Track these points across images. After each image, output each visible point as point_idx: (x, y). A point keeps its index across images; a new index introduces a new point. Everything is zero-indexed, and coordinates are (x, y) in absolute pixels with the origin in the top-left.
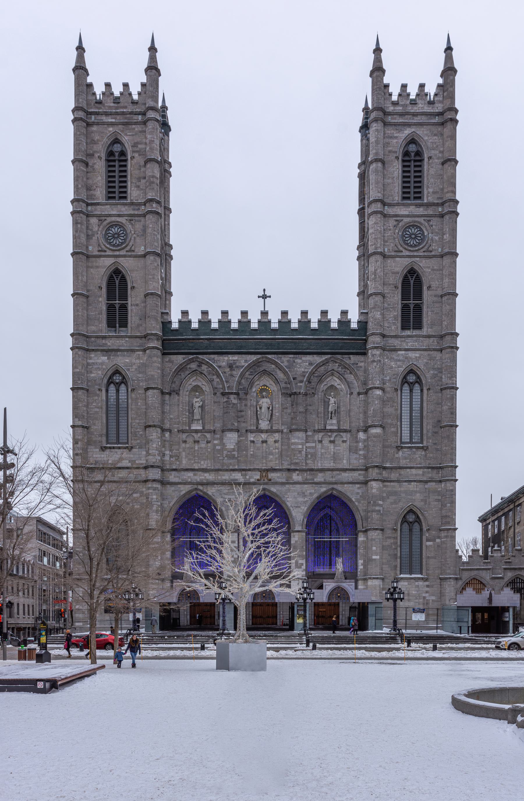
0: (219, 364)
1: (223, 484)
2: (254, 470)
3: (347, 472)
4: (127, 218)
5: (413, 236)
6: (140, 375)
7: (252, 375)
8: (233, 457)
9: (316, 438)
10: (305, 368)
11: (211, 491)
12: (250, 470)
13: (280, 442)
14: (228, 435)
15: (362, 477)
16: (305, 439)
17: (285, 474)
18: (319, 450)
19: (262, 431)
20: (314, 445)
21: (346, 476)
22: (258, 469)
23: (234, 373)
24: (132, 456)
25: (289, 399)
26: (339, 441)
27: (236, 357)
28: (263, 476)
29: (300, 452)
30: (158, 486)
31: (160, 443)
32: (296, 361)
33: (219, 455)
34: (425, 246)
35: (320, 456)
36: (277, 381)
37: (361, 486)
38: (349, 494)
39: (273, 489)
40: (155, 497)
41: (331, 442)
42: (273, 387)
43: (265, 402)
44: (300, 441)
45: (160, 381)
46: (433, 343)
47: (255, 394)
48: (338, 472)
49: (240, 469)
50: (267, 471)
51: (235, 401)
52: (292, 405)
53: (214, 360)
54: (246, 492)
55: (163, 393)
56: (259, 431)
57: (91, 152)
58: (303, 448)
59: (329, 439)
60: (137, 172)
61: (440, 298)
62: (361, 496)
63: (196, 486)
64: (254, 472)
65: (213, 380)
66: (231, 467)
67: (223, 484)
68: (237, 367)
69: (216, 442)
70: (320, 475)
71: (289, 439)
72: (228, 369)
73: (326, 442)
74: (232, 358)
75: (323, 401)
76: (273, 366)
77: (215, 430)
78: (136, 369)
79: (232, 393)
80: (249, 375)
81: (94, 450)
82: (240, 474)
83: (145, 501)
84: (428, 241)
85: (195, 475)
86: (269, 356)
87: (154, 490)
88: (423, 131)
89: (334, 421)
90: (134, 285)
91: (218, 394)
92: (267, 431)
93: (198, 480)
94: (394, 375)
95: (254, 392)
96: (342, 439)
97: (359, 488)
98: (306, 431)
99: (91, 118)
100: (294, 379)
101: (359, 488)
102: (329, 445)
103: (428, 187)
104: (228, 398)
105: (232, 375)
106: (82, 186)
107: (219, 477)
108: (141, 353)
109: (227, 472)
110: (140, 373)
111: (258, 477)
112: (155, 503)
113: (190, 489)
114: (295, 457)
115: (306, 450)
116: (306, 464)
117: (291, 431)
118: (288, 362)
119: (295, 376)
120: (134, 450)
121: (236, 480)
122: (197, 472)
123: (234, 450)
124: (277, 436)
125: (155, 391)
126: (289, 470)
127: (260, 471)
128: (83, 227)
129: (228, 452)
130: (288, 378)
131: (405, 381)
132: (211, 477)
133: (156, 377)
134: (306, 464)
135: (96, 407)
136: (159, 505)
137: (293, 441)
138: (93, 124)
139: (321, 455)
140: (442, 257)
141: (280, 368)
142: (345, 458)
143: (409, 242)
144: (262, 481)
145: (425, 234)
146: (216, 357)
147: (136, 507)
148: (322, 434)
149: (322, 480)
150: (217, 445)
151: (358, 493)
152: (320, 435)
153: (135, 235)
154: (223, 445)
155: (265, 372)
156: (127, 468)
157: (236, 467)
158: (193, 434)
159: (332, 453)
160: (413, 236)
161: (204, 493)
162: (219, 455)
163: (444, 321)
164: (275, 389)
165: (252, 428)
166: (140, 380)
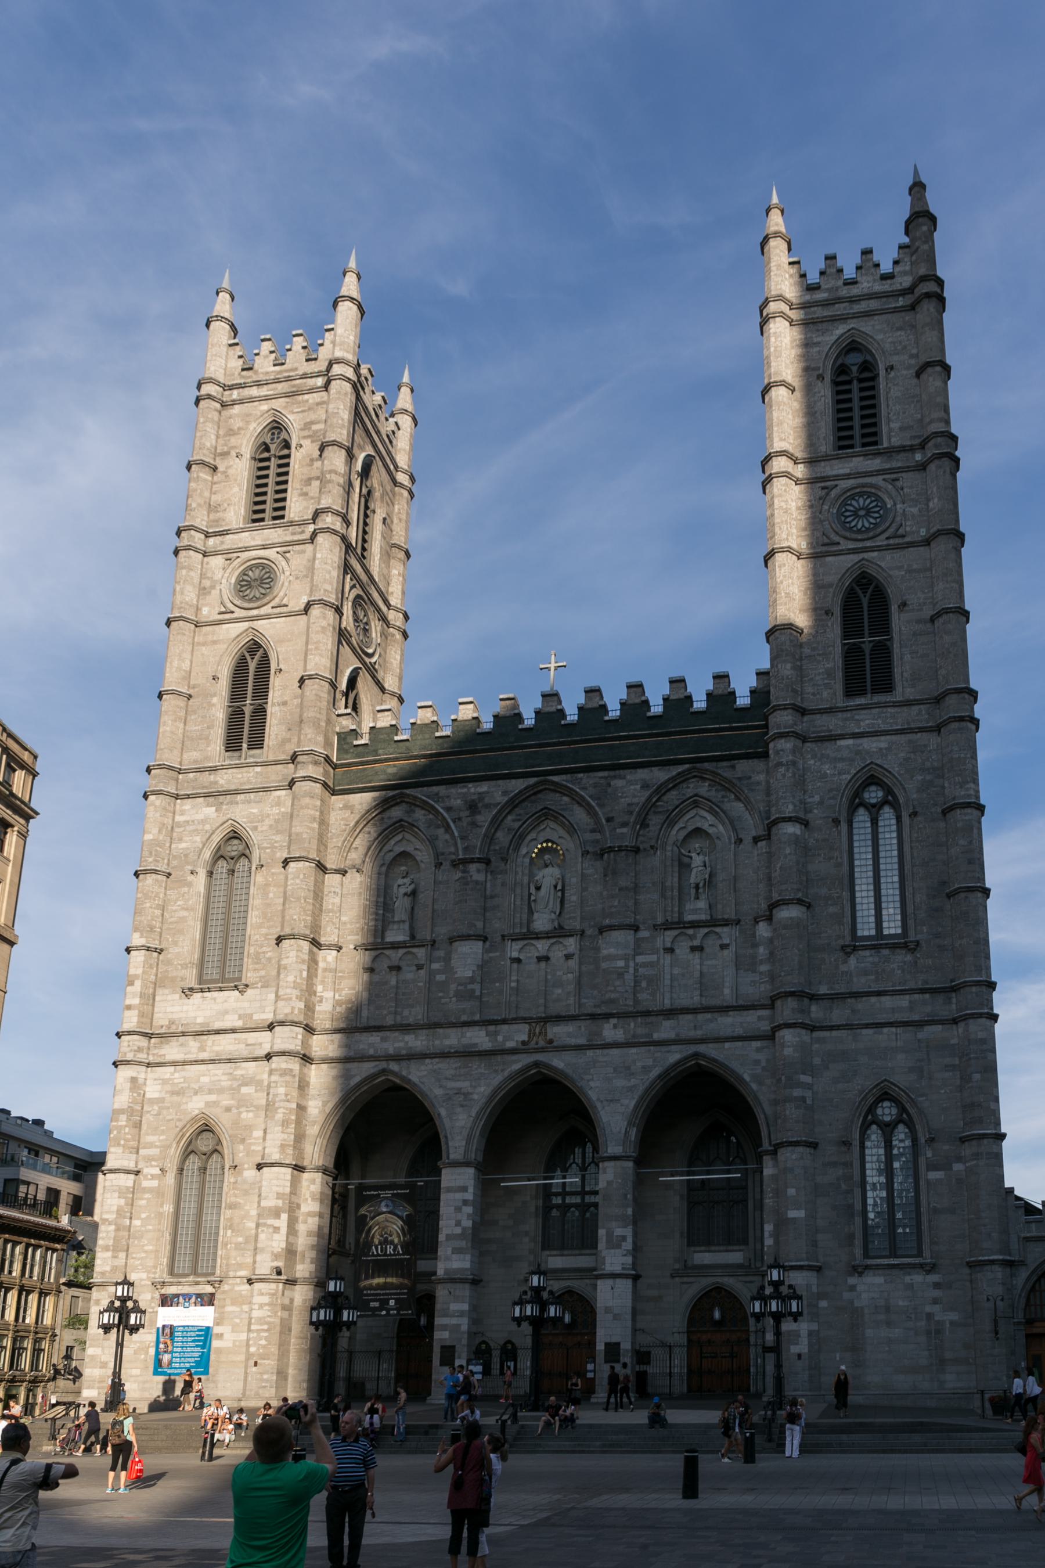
0: (448, 804)
1: (444, 1055)
2: (515, 1020)
3: (731, 1013)
4: (278, 549)
5: (862, 513)
6: (278, 838)
7: (519, 820)
8: (470, 995)
9: (659, 943)
10: (634, 796)
11: (417, 1075)
12: (504, 1021)
13: (576, 957)
14: (459, 949)
15: (767, 1022)
16: (632, 946)
17: (584, 1025)
18: (667, 969)
19: (538, 936)
20: (654, 958)
21: (728, 1024)
22: (524, 1019)
23: (479, 818)
24: (246, 1005)
25: (598, 863)
26: (712, 945)
27: (484, 787)
28: (534, 1034)
29: (621, 975)
30: (295, 1065)
31: (305, 974)
32: (612, 783)
33: (441, 994)
34: (888, 528)
35: (667, 982)
36: (571, 829)
37: (765, 1043)
38: (735, 1065)
39: (558, 1062)
40: (282, 1090)
41: (693, 949)
42: (567, 844)
43: (548, 876)
44: (620, 952)
45: (314, 845)
46: (918, 715)
47: (527, 860)
48: (709, 1016)
49: (484, 1021)
50: (545, 1023)
51: (480, 877)
52: (605, 875)
53: (437, 797)
54: (496, 1071)
55: (321, 867)
56: (531, 935)
57: (226, 449)
58: (627, 966)
59: (691, 944)
60: (305, 470)
61: (929, 625)
62: (764, 1069)
63: (383, 1065)
64: (515, 1027)
65: (437, 839)
66: (464, 1018)
67: (444, 1055)
68: (488, 806)
69: (435, 966)
70: (667, 1024)
71: (597, 949)
72: (467, 813)
73: (682, 950)
74: (474, 789)
75: (676, 864)
76: (566, 799)
77: (434, 941)
78: (271, 826)
79: (472, 861)
80: (514, 821)
81: (170, 997)
82: (483, 1033)
83: (264, 1102)
84: (894, 517)
85: (384, 1039)
86: (555, 778)
87: (281, 1075)
88: (873, 326)
89: (702, 904)
90: (281, 666)
91: (446, 865)
92: (547, 936)
93: (391, 1051)
94: (830, 791)
95: (524, 856)
96: (720, 942)
97: (758, 1050)
98: (636, 928)
99: (231, 395)
100: (609, 820)
101: (758, 1050)
102: (691, 956)
103: (889, 420)
104: (464, 872)
105: (474, 824)
106: (199, 505)
107: (437, 1042)
108: (283, 792)
109: (454, 1030)
110: (278, 832)
111: (525, 1038)
112: (282, 1104)
113: (372, 1071)
114: (610, 988)
115: (636, 970)
116: (636, 1001)
117: (601, 932)
118: (595, 787)
119: (611, 815)
120: (249, 992)
121: (476, 1045)
122: (388, 1033)
123: (472, 980)
124: (571, 944)
125: (301, 864)
126: (593, 1017)
127: (529, 1024)
128: (192, 574)
129: (460, 984)
130: (597, 821)
131: (856, 802)
132: (419, 1043)
133: (305, 836)
134: (636, 1001)
135: (183, 909)
136: (291, 1109)
137: (605, 952)
138: (234, 403)
139: (671, 980)
140: (929, 544)
141: (581, 802)
142: (727, 984)
143: (853, 524)
144: (532, 1044)
145: (889, 506)
146: (441, 790)
147: (244, 1115)
148: (675, 932)
149: (672, 1035)
150: (439, 972)
151: (757, 1062)
152: (670, 934)
153: (291, 578)
154: (448, 969)
155: (547, 814)
156: (234, 1031)
157: (477, 1017)
158: (387, 952)
159: (697, 974)
160: (862, 513)
161: (403, 1078)
162: (441, 994)
163: (941, 667)
164: (571, 846)
165: (517, 931)
166: (276, 847)
